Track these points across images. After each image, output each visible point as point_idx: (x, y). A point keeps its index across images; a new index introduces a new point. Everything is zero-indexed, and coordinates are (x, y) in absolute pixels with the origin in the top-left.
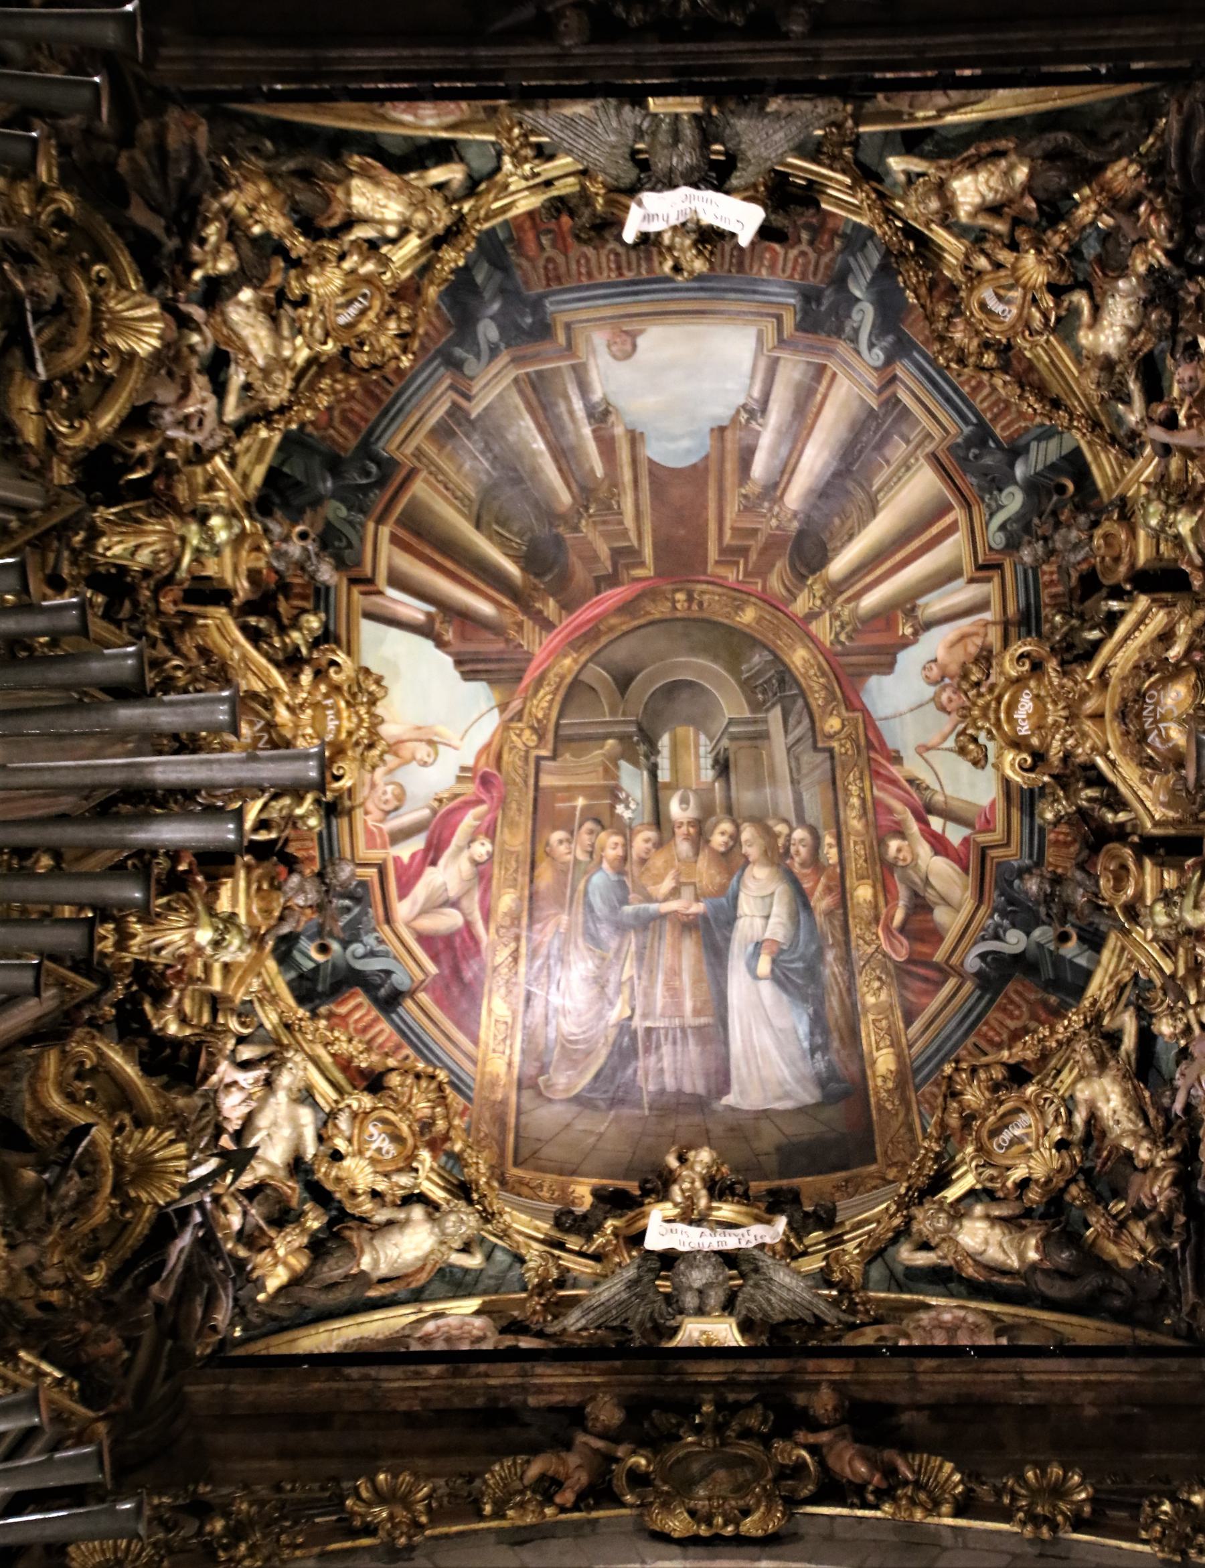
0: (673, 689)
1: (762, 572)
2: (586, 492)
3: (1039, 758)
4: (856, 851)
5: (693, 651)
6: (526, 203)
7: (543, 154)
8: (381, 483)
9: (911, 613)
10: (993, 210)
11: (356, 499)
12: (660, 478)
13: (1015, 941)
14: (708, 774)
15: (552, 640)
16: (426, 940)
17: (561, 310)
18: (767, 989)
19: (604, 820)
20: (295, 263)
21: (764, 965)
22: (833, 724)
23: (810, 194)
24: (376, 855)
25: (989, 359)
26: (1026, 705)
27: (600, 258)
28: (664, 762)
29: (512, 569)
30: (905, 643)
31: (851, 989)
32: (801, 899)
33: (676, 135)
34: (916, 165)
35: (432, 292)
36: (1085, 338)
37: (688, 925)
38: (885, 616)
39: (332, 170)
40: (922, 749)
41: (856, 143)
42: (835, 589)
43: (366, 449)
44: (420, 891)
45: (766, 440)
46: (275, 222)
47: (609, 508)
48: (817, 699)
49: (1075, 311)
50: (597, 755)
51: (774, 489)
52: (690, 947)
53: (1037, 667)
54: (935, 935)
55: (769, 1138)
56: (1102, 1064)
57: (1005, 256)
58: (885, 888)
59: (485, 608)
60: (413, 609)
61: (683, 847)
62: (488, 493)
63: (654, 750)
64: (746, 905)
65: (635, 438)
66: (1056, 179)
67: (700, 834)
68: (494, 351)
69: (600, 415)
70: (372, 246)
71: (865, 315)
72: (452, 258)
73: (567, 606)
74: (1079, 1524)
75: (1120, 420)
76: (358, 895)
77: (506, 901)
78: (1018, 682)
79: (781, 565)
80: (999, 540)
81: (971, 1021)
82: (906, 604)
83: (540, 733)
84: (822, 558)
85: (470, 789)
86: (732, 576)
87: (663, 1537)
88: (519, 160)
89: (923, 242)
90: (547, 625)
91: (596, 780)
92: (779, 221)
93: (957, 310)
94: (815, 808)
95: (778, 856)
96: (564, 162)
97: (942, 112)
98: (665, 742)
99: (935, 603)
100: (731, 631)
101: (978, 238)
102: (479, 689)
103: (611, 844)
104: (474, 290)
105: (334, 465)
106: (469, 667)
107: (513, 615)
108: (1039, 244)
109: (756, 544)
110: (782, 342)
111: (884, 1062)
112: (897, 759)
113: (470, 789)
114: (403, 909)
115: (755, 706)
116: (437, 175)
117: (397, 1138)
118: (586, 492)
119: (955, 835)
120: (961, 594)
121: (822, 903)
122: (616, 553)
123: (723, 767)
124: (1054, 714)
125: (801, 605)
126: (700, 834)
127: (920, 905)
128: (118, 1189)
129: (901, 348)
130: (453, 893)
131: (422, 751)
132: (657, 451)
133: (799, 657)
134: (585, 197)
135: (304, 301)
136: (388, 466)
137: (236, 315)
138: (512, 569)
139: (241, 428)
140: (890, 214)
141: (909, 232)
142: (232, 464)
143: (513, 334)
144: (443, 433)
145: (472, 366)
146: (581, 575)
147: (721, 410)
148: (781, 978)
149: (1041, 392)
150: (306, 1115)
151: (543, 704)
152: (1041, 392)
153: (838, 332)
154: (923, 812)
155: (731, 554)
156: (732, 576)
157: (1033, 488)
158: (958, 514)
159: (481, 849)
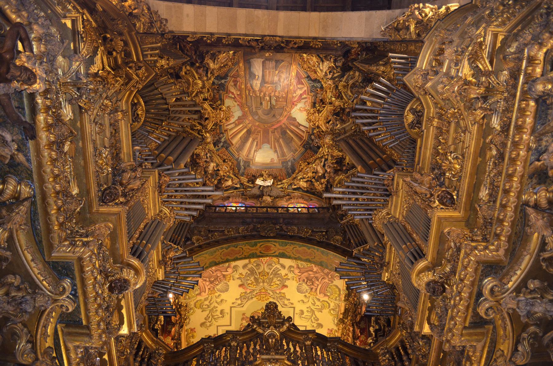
0: (268, 114)
1: (255, 129)
2: (278, 141)
3: (220, 109)
4: (244, 92)
5: (264, 119)
6: (284, 181)
7: (282, 188)
8: (305, 145)
9: (236, 124)
10: (226, 180)
11: (308, 143)
12: (268, 142)
13: (223, 81)
14: (263, 103)
15: (283, 122)
16: (303, 84)
17: (280, 166)
18: (257, 74)
19: (277, 97)
20: (314, 178)
21: (257, 77)
22: (246, 109)
23: (248, 182)
24: (309, 96)
25: (226, 160)
26: (222, 116)
27: (275, 172)
28: (269, 105)
29: (288, 132)
30: (237, 120)
31: (245, 74)
32: (252, 86)
33: (266, 193)
34: (236, 186)
35: (297, 171)
36: (215, 165)
37: (267, 83)
38: (239, 124)
39: (309, 189)
40: (235, 106)
41: (243, 188)
42: (245, 127)
43: (306, 149)
44: (303, 90)
45: (254, 147)
46: (316, 184)
47: (276, 139)
48: (248, 112)
49: (216, 167)
50: (278, 106)
51: (254, 140)
52: (267, 80)
53: (220, 121)
54: (233, 81)
55: (257, 55)
56: (213, 70)
57: (225, 174)
58: (240, 87)
59: (292, 127)
60: (301, 128)
61: (267, 93)
62: (291, 142)
63: (270, 107)
64: (259, 85)
65: (271, 148)
66: (219, 186)
67: (265, 94)
68: (289, 161)
69: (276, 151)
70: (304, 178)
71: (242, 164)
72: (294, 176)
73: (281, 126)
74: (224, 38)
75: (210, 153)
76: (311, 91)
77: (291, 88)
78: (223, 119)
79: (253, 130)
80: (225, 134)
81: (229, 71)
82: (237, 125)
83: (286, 110)
84: (247, 131)
85: (295, 103)
86: (259, 129)
87: (280, 37)
88: (285, 187)
89: (235, 175)
90: (284, 124)
91: (279, 103)
92: (253, 178)
93: (231, 167)
94: (249, 98)
95: (254, 91)
96: (279, 186)
97: (233, 192)
98: (269, 107)
99: (233, 126)
100: (259, 122)
101: (229, 177)
102: (294, 116)
103: (277, 94)
104: (291, 169)
105: (310, 148)
106: (295, 119)
107: (288, 125)
108: (221, 176)
109: (256, 133)
110: (252, 160)
111: (241, 65)
112: (238, 105)
113: (295, 103)
114: (306, 88)
115: (257, 112)
116: (295, 187)
117: (309, 62)
118: (278, 141)
119: (231, 95)
120: (229, 127)
121: (249, 85)
122: (274, 133)
123: (261, 104)
124: (218, 116)
125: (250, 125)
126: (265, 94)
127: (235, 85)
128: (348, 85)
129: (237, 160)
130: (299, 90)
131: (302, 109)
132: (269, 146)
133: (250, 118)
134: (277, 182)
135: (313, 172)
136: (303, 147)
137: (321, 172)
138: (288, 132)
139: (322, 157)
140: (239, 179)
141: (237, 177)
142: (323, 153)
143: (287, 162)
144: (296, 150)
145: (292, 159)
146: (279, 130)
147: (260, 151)
148: (255, 76)
149: (220, 156)
150: (321, 68)
151: (285, 113)
152: (220, 156)
153: (245, 162)
154: (235, 98)
155: (259, 132)
156: (259, 129)
157: (221, 142)
158: (230, 138)
159: (295, 95)
